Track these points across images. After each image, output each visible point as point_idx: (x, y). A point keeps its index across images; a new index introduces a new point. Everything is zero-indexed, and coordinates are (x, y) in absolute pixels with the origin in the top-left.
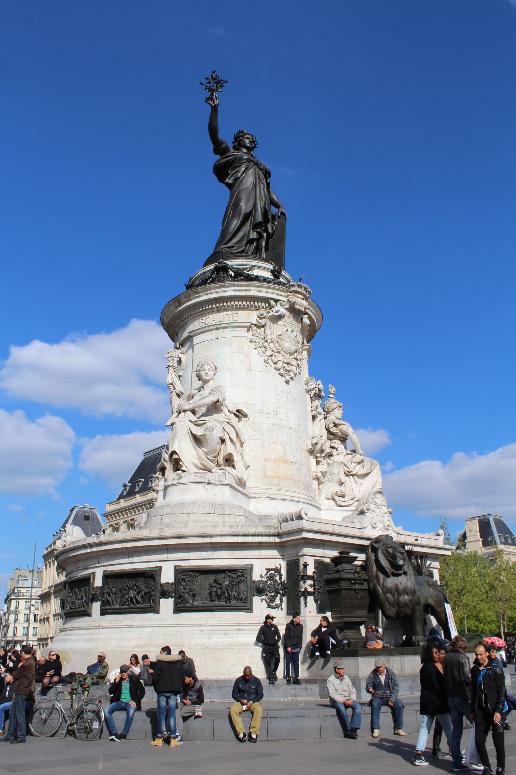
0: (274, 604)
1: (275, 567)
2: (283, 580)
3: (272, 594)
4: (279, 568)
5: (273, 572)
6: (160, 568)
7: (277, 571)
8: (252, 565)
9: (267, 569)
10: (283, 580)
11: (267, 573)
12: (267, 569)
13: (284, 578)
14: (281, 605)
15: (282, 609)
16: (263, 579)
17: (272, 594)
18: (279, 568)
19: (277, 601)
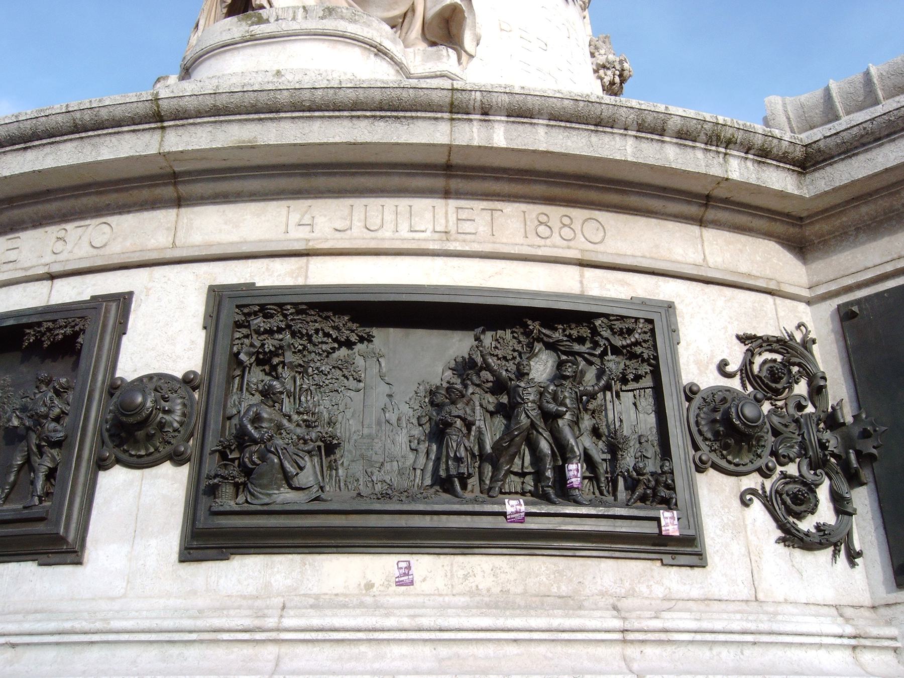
0: (807, 525)
3: (792, 469)
6: (124, 301)
8: (669, 307)
9: (743, 339)
11: (751, 353)
12: (743, 339)
13: (839, 391)
14: (849, 534)
16: (735, 384)
17: (792, 469)
19: (826, 513)
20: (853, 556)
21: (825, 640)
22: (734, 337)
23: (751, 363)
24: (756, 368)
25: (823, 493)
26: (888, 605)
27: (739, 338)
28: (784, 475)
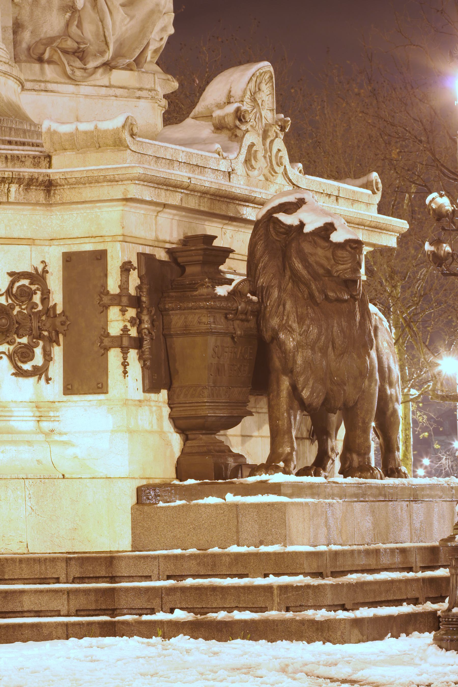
0: (27, 367)
1: (29, 269)
2: (51, 304)
3: (24, 340)
4: (40, 270)
5: (26, 282)
7: (38, 277)
9: (11, 274)
10: (51, 304)
11: (12, 283)
12: (11, 274)
13: (57, 298)
14: (47, 370)
15: (48, 380)
18: (40, 270)
19: (38, 360)
20: (48, 380)
21: (24, 419)
22: (6, 274)
23: (12, 288)
24: (15, 290)
25: (38, 351)
26: (59, 402)
27: (8, 273)
28: (20, 343)
